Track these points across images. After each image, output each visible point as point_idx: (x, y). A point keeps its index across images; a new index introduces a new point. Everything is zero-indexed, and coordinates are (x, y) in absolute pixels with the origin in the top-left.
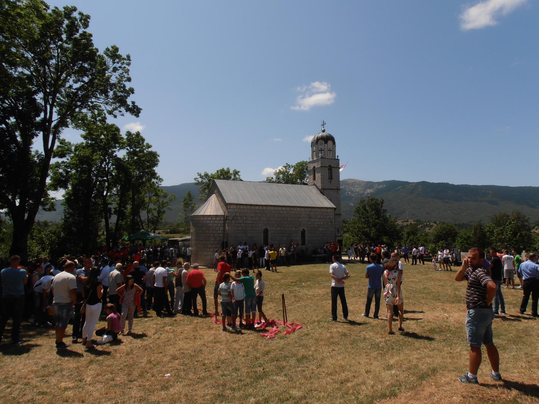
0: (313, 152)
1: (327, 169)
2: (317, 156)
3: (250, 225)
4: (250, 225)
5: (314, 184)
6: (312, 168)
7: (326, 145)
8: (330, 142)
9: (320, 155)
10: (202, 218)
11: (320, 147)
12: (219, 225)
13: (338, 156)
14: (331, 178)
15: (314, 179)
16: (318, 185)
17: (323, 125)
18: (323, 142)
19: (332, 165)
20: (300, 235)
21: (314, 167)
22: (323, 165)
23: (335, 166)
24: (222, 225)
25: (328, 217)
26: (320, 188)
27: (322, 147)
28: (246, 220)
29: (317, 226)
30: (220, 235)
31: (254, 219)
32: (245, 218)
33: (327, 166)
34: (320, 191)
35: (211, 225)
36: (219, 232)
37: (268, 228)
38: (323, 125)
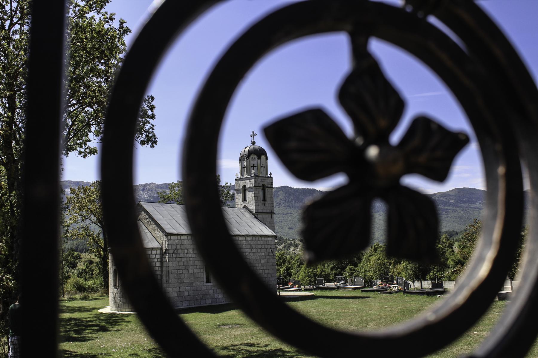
0: (242, 168)
1: (260, 190)
2: (249, 173)
3: (191, 259)
4: (191, 259)
5: (245, 207)
6: (241, 187)
7: (259, 161)
8: (263, 157)
9: (253, 172)
11: (252, 163)
13: (271, 174)
14: (264, 200)
15: (244, 200)
16: (250, 208)
21: (244, 186)
23: (269, 186)
24: (159, 260)
25: (269, 246)
26: (254, 211)
27: (255, 163)
29: (258, 258)
32: (186, 251)
34: (254, 215)
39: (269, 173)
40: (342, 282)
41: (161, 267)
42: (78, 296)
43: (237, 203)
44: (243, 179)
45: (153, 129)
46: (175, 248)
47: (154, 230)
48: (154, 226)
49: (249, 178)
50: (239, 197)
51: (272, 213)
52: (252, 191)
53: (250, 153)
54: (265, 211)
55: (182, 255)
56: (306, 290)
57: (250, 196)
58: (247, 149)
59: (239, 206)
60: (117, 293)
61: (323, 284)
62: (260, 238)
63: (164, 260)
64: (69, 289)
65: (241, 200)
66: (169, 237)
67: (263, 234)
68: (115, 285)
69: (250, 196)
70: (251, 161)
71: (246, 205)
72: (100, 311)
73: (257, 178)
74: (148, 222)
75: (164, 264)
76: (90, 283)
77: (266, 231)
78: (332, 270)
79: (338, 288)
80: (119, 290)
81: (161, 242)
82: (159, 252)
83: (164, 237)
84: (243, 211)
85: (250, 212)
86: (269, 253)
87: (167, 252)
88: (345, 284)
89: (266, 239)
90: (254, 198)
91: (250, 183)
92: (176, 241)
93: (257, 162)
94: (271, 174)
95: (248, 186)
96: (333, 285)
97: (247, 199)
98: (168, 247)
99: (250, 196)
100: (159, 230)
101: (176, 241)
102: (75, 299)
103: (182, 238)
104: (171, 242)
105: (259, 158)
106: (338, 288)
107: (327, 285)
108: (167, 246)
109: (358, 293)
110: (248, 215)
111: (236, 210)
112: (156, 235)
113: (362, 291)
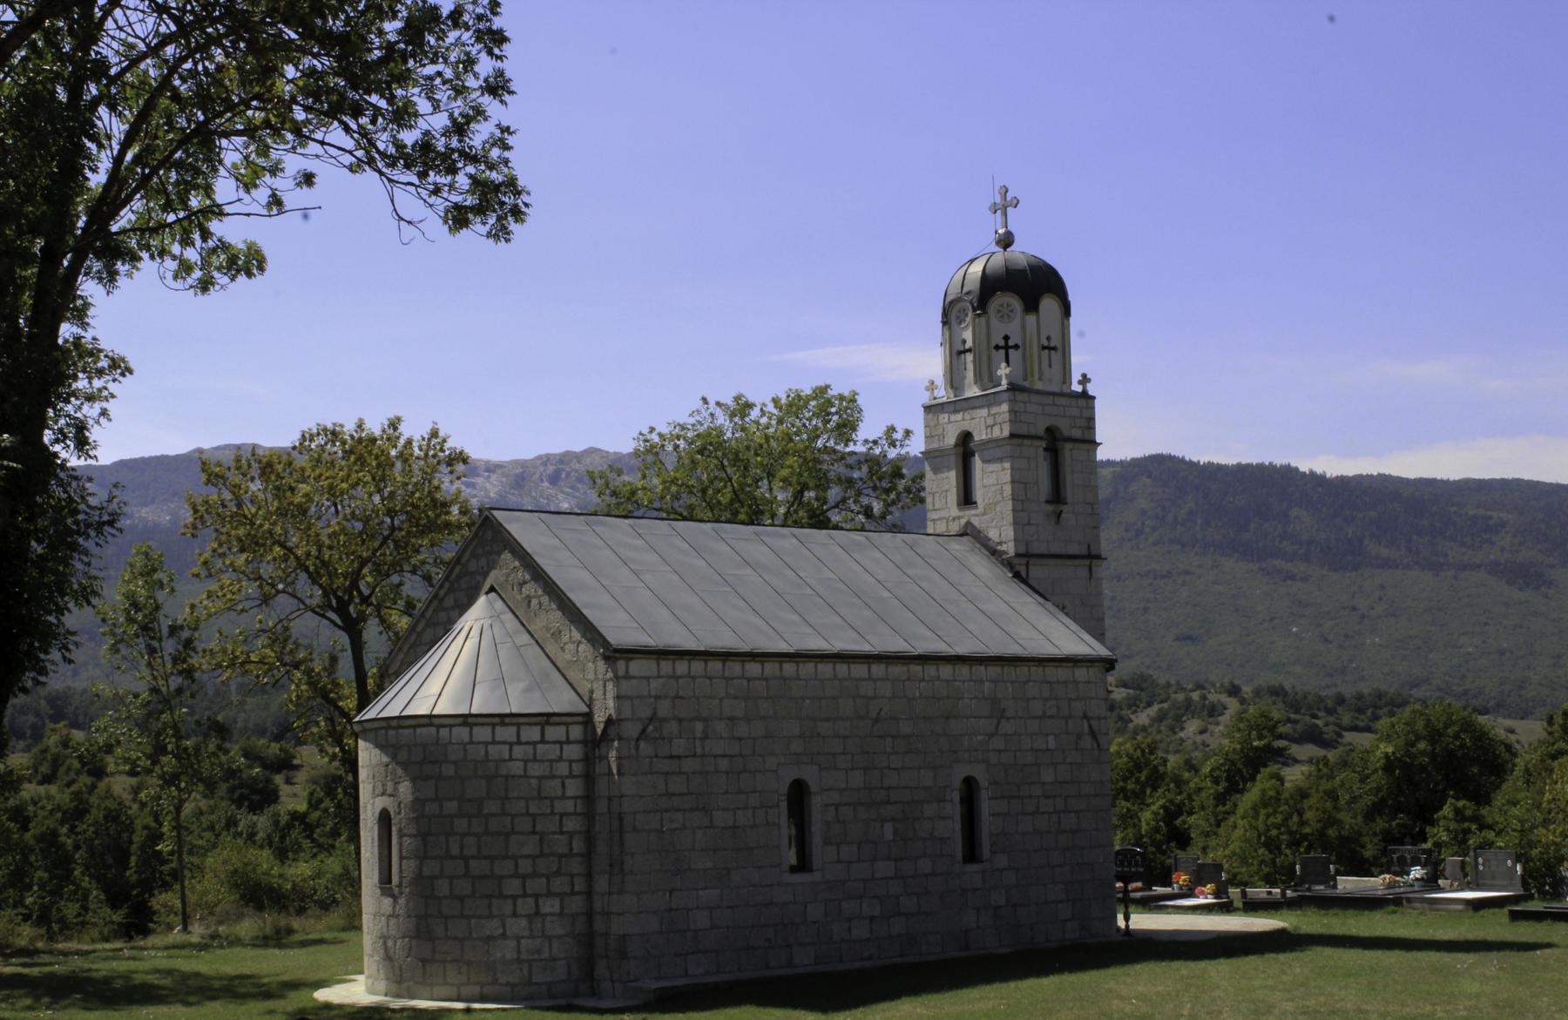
0: (956, 354)
1: (1038, 450)
2: (985, 376)
3: (724, 764)
4: (724, 764)
5: (969, 532)
6: (951, 440)
7: (1031, 319)
8: (1048, 304)
9: (1003, 371)
10: (462, 733)
11: (999, 330)
12: (562, 769)
13: (1085, 380)
14: (1057, 497)
15: (967, 499)
16: (993, 534)
17: (1005, 205)
18: (1016, 303)
19: (1066, 429)
20: (954, 809)
21: (966, 437)
22: (1023, 430)
23: (1077, 434)
24: (578, 769)
26: (1009, 548)
27: (1013, 329)
28: (705, 738)
30: (571, 825)
31: (742, 730)
32: (699, 726)
33: (1041, 431)
34: (1009, 564)
35: (516, 768)
36: (559, 807)
37: (809, 774)
38: (1005, 205)
39: (1076, 377)
40: (1417, 872)
41: (589, 798)
42: (247, 927)
43: (931, 515)
44: (959, 405)
45: (507, 148)
46: (648, 713)
47: (557, 635)
48: (555, 617)
49: (987, 401)
50: (942, 487)
51: (1092, 557)
52: (1000, 460)
53: (991, 285)
54: (1062, 551)
55: (679, 746)
56: (1252, 907)
57: (992, 479)
58: (977, 269)
59: (941, 528)
60: (393, 915)
61: (1330, 881)
62: (1036, 671)
63: (600, 768)
64: (210, 898)
65: (953, 497)
66: (621, 665)
67: (1048, 650)
68: (385, 879)
69: (992, 479)
70: (994, 322)
71: (976, 522)
72: (322, 995)
73: (1020, 397)
74: (529, 599)
75: (602, 787)
76: (301, 869)
77: (1061, 637)
78: (1371, 814)
79: (1397, 901)
80: (402, 901)
81: (584, 688)
82: (576, 732)
83: (601, 665)
84: (960, 547)
85: (994, 553)
86: (1079, 736)
87: (612, 731)
88: (1431, 882)
89: (1062, 673)
90: (1008, 490)
91: (989, 424)
92: (654, 684)
93: (1023, 326)
94: (1085, 380)
95: (980, 435)
96: (1376, 884)
97: (979, 495)
98: (618, 709)
99: (991, 480)
100: (577, 635)
101: (654, 684)
102: (235, 942)
103: (682, 667)
104: (627, 687)
105: (1031, 306)
106: (1397, 901)
107: (1348, 884)
108: (611, 703)
109: (1497, 927)
110: (982, 566)
111: (927, 545)
112: (563, 658)
113: (1515, 916)
